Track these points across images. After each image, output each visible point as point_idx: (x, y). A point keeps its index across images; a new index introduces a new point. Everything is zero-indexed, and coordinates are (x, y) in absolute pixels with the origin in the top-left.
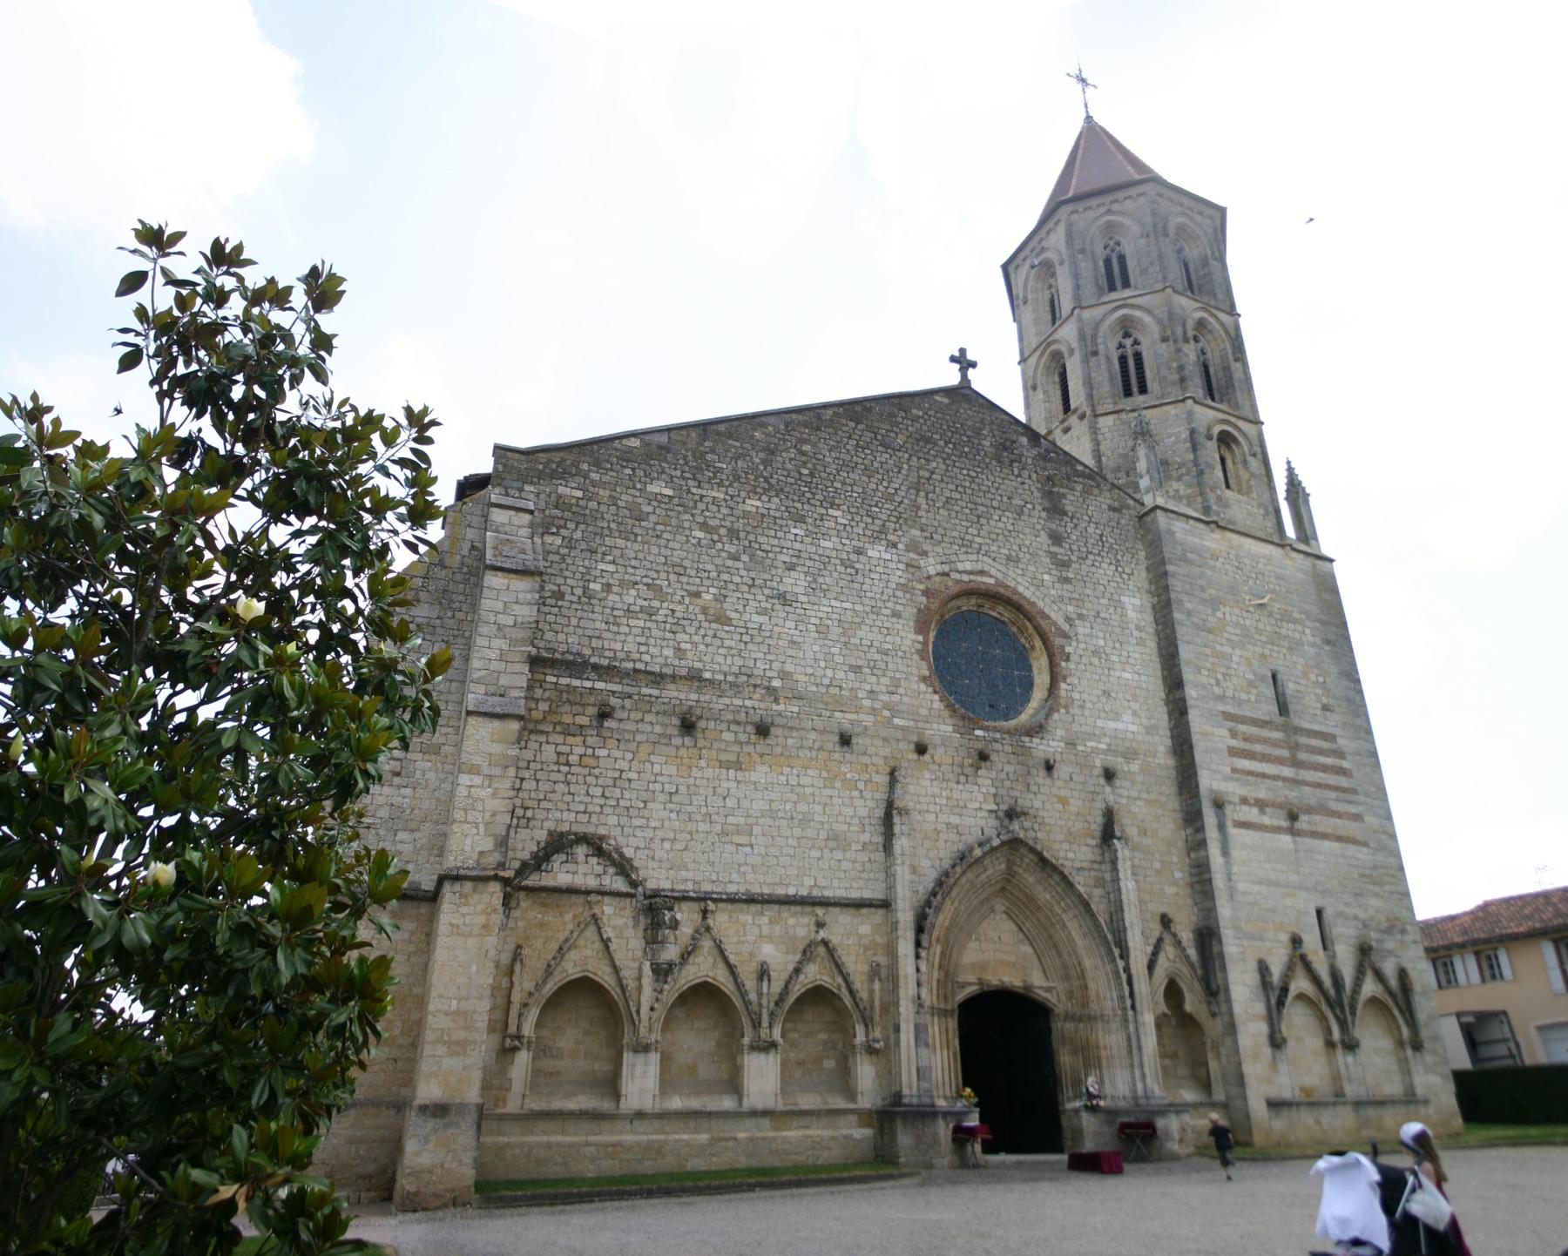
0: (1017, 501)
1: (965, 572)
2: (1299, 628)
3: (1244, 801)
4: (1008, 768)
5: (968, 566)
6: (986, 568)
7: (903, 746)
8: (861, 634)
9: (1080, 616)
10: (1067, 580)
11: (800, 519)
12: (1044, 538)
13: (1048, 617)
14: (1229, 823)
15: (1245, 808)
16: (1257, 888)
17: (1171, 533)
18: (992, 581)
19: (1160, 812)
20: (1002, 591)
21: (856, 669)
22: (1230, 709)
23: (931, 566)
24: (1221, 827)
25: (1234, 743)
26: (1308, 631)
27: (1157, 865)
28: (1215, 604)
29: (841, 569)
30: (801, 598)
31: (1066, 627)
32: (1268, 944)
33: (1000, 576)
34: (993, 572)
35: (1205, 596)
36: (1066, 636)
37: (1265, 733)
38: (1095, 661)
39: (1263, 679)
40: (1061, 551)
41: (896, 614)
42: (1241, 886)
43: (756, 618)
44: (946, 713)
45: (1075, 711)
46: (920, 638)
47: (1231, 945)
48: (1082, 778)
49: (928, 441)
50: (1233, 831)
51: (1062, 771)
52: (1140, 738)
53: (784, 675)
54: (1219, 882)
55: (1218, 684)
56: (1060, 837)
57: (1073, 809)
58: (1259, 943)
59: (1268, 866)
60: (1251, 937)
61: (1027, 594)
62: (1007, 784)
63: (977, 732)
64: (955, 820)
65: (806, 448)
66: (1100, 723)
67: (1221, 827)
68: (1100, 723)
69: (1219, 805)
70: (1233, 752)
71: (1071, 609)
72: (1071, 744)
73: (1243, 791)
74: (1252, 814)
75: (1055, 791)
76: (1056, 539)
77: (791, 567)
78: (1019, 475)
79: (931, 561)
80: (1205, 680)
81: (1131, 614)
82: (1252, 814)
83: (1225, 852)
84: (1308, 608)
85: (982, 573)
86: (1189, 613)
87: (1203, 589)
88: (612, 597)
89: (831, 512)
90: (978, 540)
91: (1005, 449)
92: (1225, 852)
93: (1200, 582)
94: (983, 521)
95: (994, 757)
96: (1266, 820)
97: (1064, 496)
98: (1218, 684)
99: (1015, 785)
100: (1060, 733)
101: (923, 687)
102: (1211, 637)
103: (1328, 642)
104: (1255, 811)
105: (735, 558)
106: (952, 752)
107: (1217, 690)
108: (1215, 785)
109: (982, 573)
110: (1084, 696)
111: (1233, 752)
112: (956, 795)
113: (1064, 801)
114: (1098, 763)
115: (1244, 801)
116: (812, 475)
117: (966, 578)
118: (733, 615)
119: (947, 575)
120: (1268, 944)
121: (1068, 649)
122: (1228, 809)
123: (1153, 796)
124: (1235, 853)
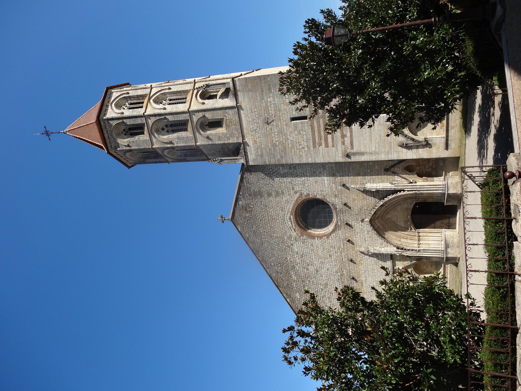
0: (262, 206)
1: (292, 224)
2: (269, 104)
3: (343, 143)
4: (347, 215)
5: (290, 223)
6: (288, 218)
7: (348, 245)
8: (320, 254)
9: (293, 189)
10: (283, 193)
11: (294, 267)
12: (271, 198)
13: (297, 199)
14: (352, 151)
15: (346, 143)
16: (373, 142)
17: (254, 160)
18: (292, 216)
19: (351, 168)
20: (294, 214)
21: (330, 256)
22: (311, 144)
23: (294, 234)
24: (355, 154)
25: (323, 144)
26: (269, 100)
27: (369, 171)
28: (274, 145)
29: (304, 258)
30: (315, 267)
31: (298, 195)
32: (392, 140)
33: (289, 214)
34: (289, 216)
35: (272, 148)
36: (301, 194)
37: (316, 129)
38: (306, 185)
39: (296, 126)
40: (273, 193)
41: (312, 245)
42: (374, 149)
43: (324, 277)
44: (336, 232)
45: (325, 193)
46: (316, 238)
47: (394, 156)
48: (346, 194)
49: (255, 232)
50: (355, 150)
51: (345, 200)
52: (328, 172)
53: (337, 272)
54: (373, 158)
55: (303, 148)
56: (365, 202)
57: (356, 197)
58: (392, 144)
59: (364, 136)
60: (390, 148)
61: (292, 206)
62: (352, 216)
63: (339, 224)
64: (366, 233)
65: (272, 264)
66: (327, 186)
67: (355, 154)
68: (327, 186)
69: (348, 156)
70: (327, 146)
71: (292, 192)
72: (336, 196)
73: (340, 143)
74: (347, 140)
75: (351, 202)
76: (270, 195)
77: (308, 269)
78: (253, 205)
79: (292, 233)
80: (304, 154)
81: (286, 171)
82: (347, 140)
83: (362, 154)
84: (259, 98)
85: (290, 219)
86: (281, 157)
87: (270, 149)
88: (328, 305)
89: (288, 259)
90: (280, 220)
91: (246, 209)
92: (362, 154)
93: (268, 151)
94: (273, 217)
95: (345, 220)
96: (348, 134)
97: (254, 191)
98: (303, 148)
99: (352, 214)
100: (333, 199)
101: (330, 238)
102: (287, 148)
103: (270, 89)
104: (346, 139)
105: (309, 281)
106: (347, 231)
107: (306, 149)
108: (340, 155)
109: (290, 219)
110: (319, 190)
111: (327, 146)
112: (359, 231)
113: (354, 200)
114: (339, 187)
115: (343, 143)
116: (280, 263)
117: (294, 224)
118: (324, 282)
119: (295, 230)
120: (392, 140)
121: (305, 194)
122: (349, 151)
123: (346, 169)
124: (363, 150)
